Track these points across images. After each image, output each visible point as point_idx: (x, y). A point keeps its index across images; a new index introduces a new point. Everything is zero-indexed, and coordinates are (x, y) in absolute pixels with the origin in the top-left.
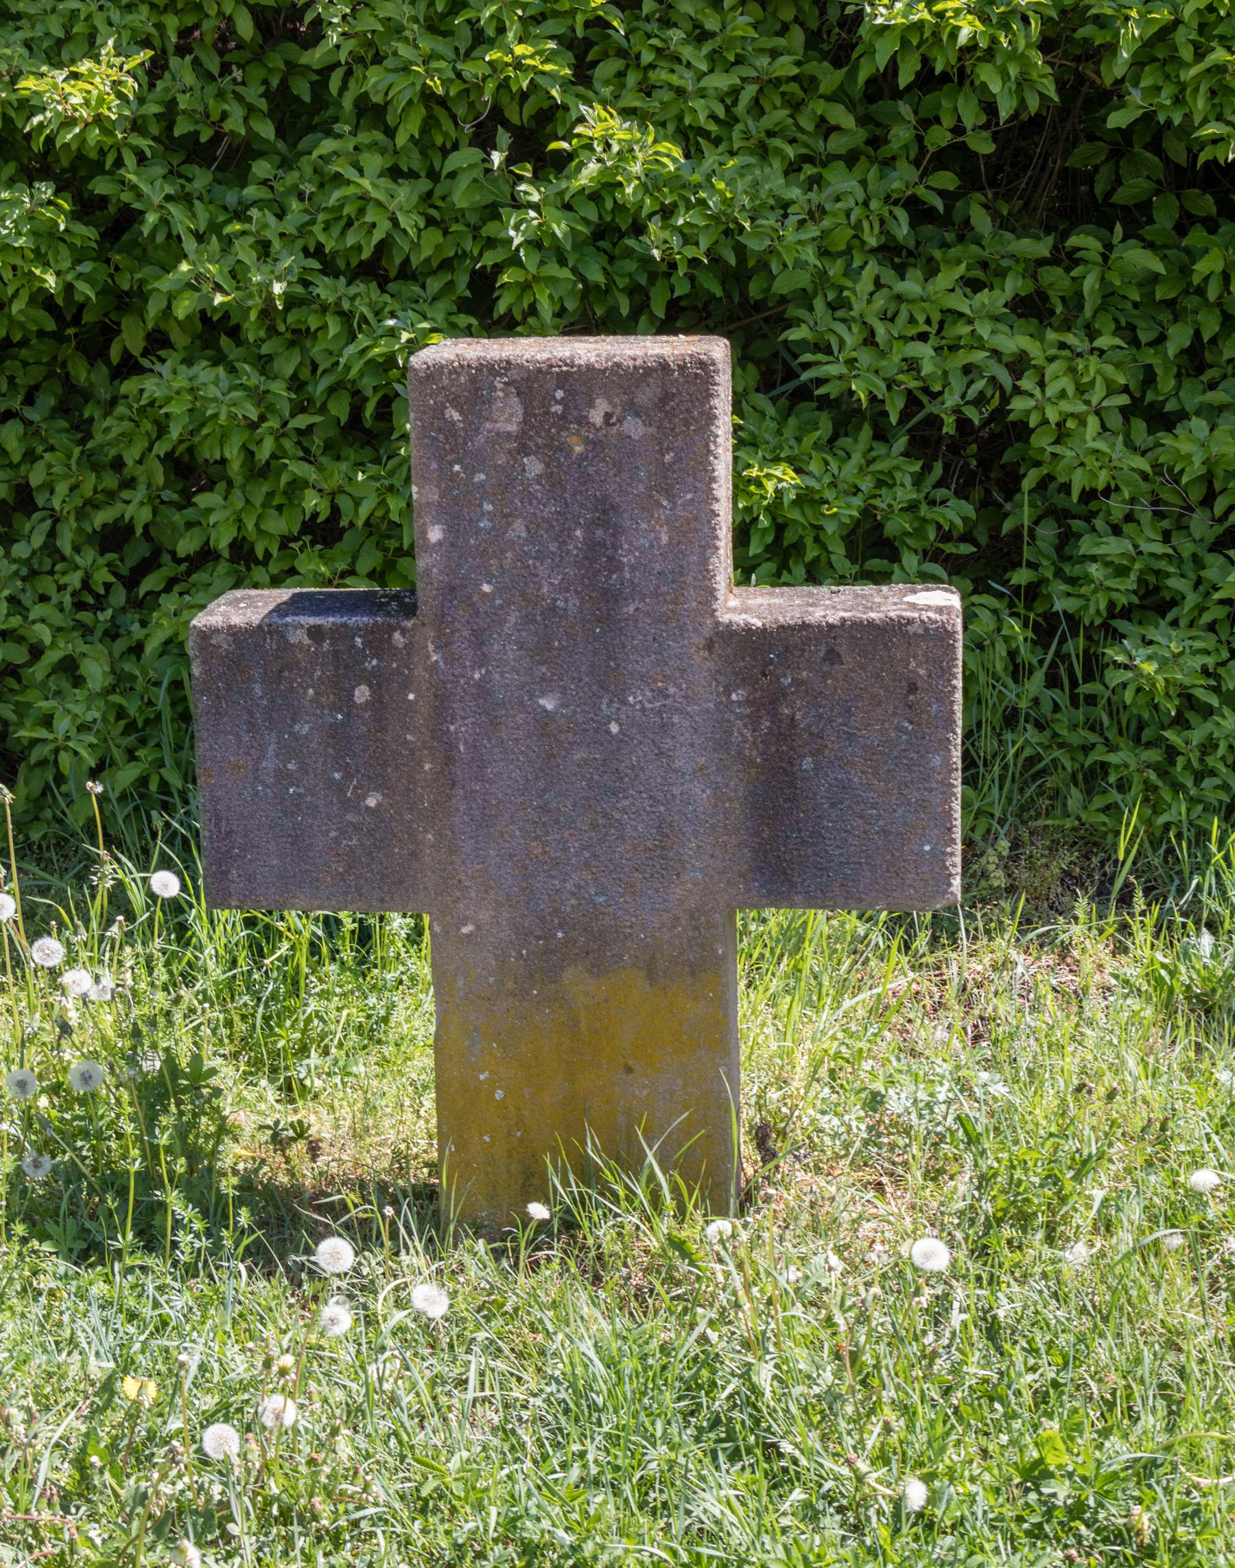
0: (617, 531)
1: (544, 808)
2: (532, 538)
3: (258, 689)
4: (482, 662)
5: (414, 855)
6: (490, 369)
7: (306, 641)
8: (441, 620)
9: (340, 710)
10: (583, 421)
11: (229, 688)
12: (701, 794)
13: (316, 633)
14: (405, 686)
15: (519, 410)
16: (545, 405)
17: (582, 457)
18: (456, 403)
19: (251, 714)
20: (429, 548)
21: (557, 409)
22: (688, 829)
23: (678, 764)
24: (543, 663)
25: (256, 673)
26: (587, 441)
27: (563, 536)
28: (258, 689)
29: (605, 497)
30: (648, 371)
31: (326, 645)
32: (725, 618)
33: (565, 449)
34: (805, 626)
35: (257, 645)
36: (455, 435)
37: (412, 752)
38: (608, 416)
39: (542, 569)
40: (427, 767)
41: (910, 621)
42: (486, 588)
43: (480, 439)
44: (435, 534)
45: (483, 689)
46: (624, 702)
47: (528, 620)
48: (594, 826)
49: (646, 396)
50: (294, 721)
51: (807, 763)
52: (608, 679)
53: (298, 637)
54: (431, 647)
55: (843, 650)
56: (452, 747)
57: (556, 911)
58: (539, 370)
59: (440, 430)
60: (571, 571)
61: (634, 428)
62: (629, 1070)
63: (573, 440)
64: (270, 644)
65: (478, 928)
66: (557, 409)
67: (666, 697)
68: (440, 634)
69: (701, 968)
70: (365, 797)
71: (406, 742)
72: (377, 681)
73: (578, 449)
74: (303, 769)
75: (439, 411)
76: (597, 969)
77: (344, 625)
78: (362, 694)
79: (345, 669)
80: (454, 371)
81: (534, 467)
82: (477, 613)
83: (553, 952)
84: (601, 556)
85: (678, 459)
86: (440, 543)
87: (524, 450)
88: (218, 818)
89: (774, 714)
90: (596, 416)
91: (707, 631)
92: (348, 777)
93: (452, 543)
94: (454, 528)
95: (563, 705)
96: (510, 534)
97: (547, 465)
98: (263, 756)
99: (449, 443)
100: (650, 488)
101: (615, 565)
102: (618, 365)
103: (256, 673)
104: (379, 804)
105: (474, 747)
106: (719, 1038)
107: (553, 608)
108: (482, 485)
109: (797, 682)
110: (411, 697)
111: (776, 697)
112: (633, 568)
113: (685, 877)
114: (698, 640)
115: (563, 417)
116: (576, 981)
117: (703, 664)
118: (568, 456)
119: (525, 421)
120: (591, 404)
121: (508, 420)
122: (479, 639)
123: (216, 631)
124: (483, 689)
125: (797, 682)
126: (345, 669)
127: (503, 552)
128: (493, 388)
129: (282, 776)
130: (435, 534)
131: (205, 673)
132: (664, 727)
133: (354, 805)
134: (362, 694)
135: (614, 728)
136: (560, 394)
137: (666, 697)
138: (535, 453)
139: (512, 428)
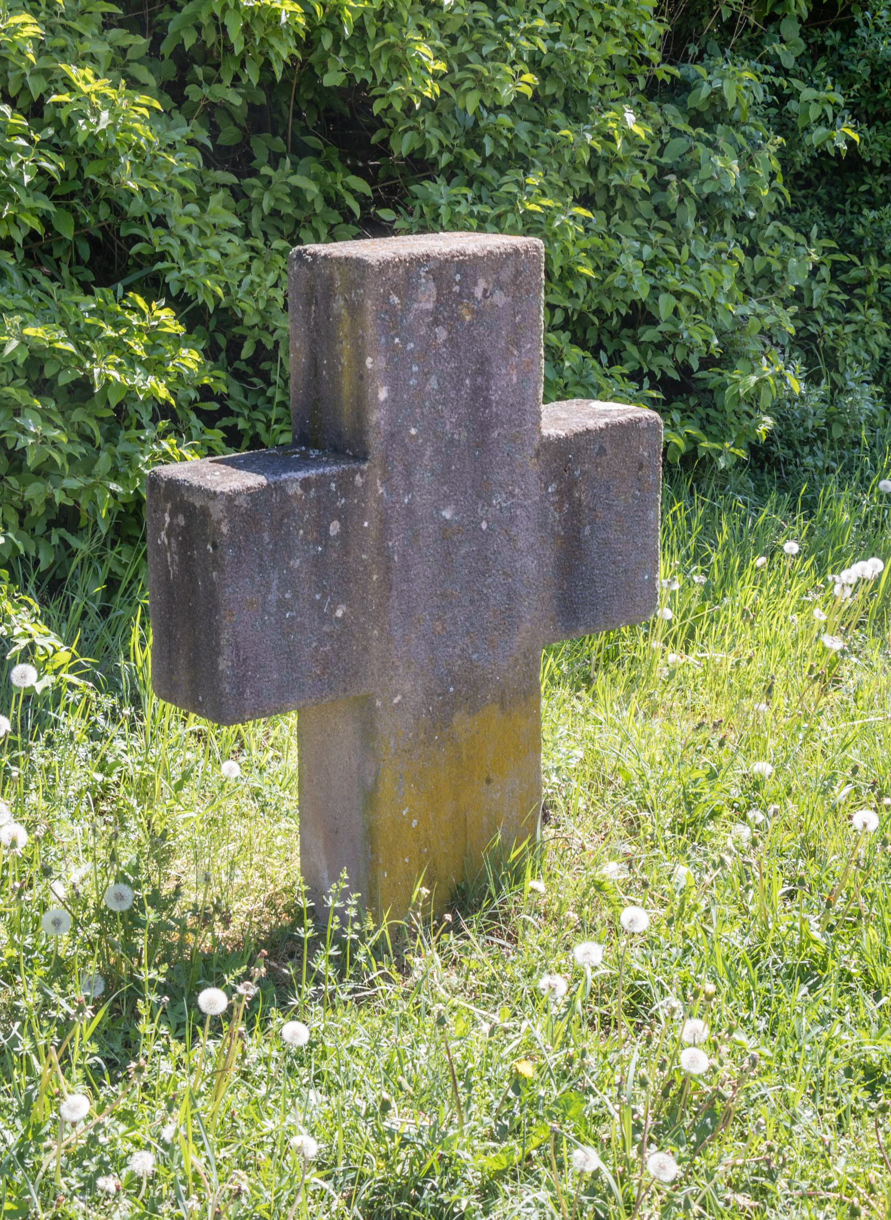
0: (488, 377)
1: (444, 596)
2: (441, 390)
3: (266, 537)
4: (409, 489)
5: (366, 649)
6: (418, 262)
7: (300, 492)
8: (386, 460)
9: (320, 544)
10: (471, 296)
11: (247, 539)
12: (531, 563)
13: (306, 484)
14: (362, 518)
15: (434, 291)
16: (449, 287)
17: (471, 324)
18: (396, 289)
19: (261, 559)
20: (378, 405)
21: (456, 289)
22: (524, 593)
23: (520, 545)
24: (443, 484)
25: (266, 523)
26: (473, 312)
27: (458, 385)
28: (266, 537)
29: (483, 352)
30: (509, 255)
31: (312, 493)
32: (545, 432)
33: (460, 318)
34: (588, 431)
35: (267, 500)
36: (395, 315)
37: (365, 567)
38: (485, 291)
39: (446, 413)
40: (375, 577)
41: (640, 420)
42: (413, 431)
43: (411, 316)
44: (383, 394)
45: (410, 510)
46: (490, 505)
47: (437, 451)
48: (472, 602)
49: (506, 275)
50: (290, 558)
51: (587, 531)
52: (482, 491)
53: (294, 489)
54: (379, 482)
55: (607, 446)
56: (390, 559)
57: (450, 672)
58: (446, 260)
59: (386, 312)
60: (463, 411)
61: (500, 299)
62: (488, 781)
63: (464, 311)
64: (276, 498)
65: (404, 697)
66: (456, 289)
67: (513, 496)
68: (385, 471)
69: (524, 696)
70: (335, 610)
71: (363, 561)
72: (344, 516)
73: (468, 318)
74: (296, 597)
75: (386, 298)
76: (473, 711)
77: (323, 475)
78: (335, 528)
79: (325, 509)
80: (396, 266)
81: (442, 334)
82: (407, 452)
83: (448, 703)
84: (480, 396)
85: (524, 319)
86: (386, 401)
87: (436, 322)
88: (237, 648)
89: (570, 496)
90: (478, 293)
91: (536, 444)
92: (324, 597)
93: (393, 400)
94: (394, 390)
95: (457, 514)
96: (428, 388)
97: (450, 333)
98: (269, 591)
99: (392, 321)
100: (507, 343)
101: (487, 403)
102: (491, 252)
103: (266, 523)
104: (344, 614)
105: (403, 556)
106: (532, 742)
107: (452, 441)
108: (412, 351)
109: (583, 473)
110: (366, 524)
111: (573, 484)
112: (498, 403)
113: (522, 628)
114: (531, 452)
115: (460, 295)
116: (461, 722)
117: (533, 467)
118: (462, 324)
119: (438, 301)
120: (475, 284)
121: (428, 301)
122: (408, 472)
123: (238, 494)
124: (410, 510)
125: (583, 473)
126: (325, 509)
127: (424, 401)
128: (419, 277)
129: (282, 605)
130: (383, 394)
131: (231, 530)
132: (512, 519)
133: (326, 618)
134: (335, 528)
135: (484, 526)
136: (458, 277)
137: (513, 496)
138: (443, 324)
139: (430, 306)
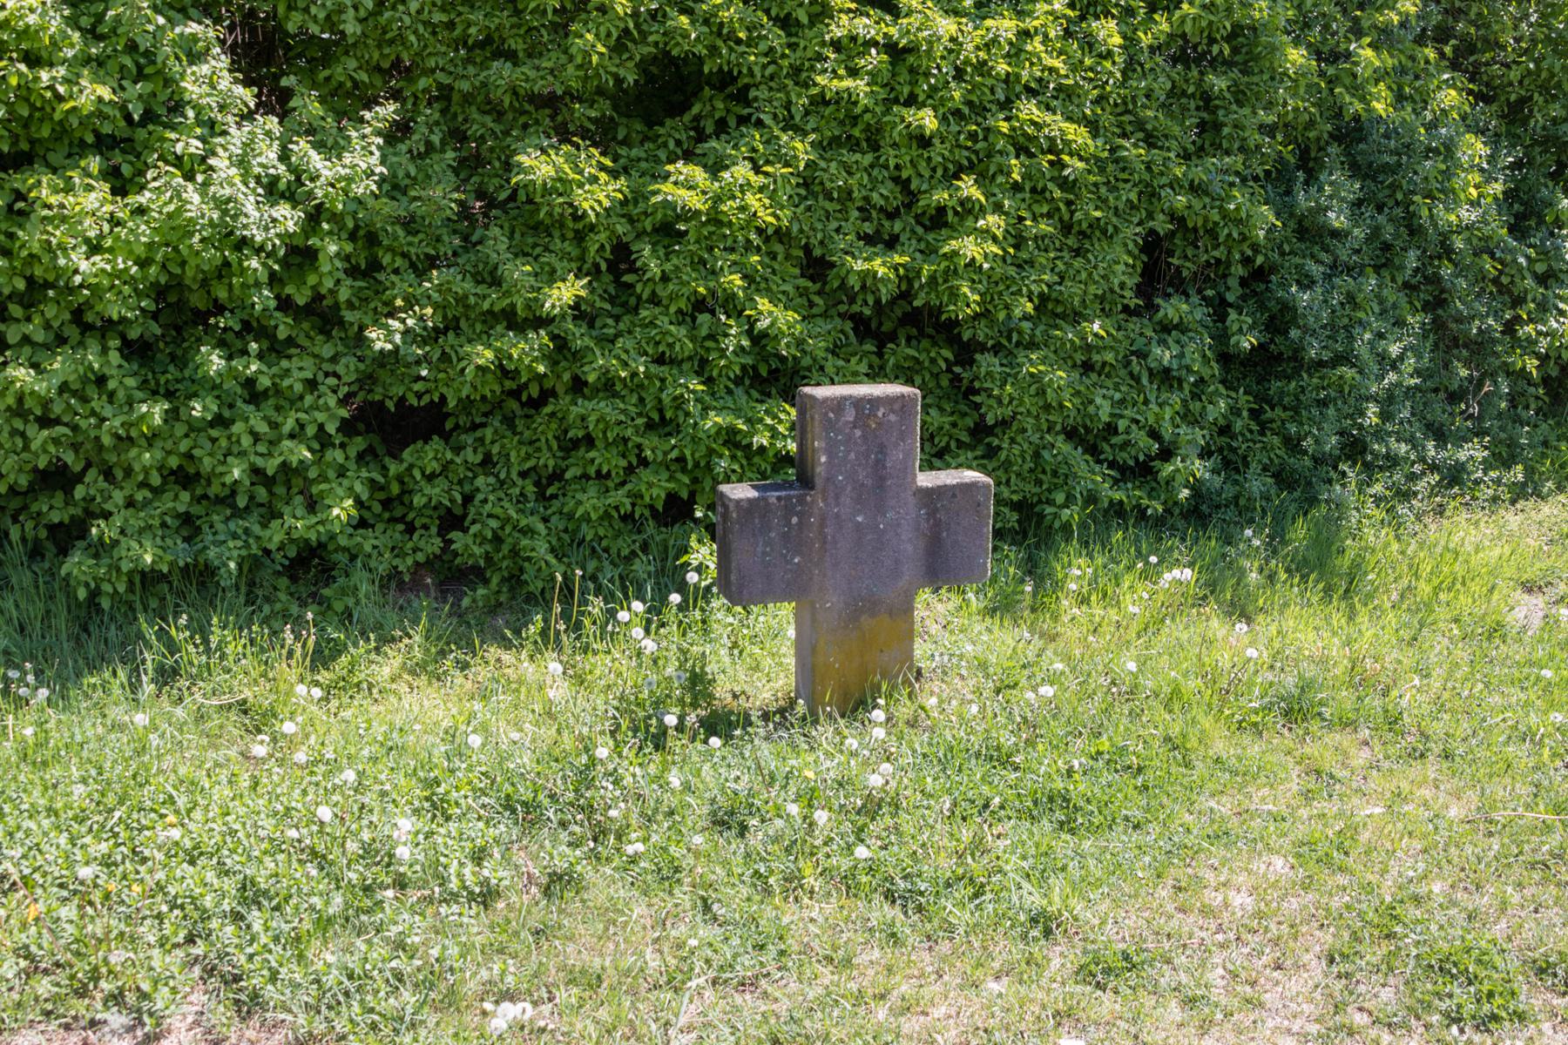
0: (885, 455)
4: (838, 505)
6: (844, 398)
8: (824, 491)
12: (910, 548)
13: (779, 498)
27: (867, 457)
44: (823, 459)
45: (837, 516)
49: (896, 407)
52: (881, 509)
53: (773, 500)
61: (893, 418)
72: (800, 515)
78: (795, 520)
79: (789, 510)
81: (858, 433)
84: (879, 464)
90: (880, 414)
93: (829, 462)
94: (830, 457)
99: (829, 426)
101: (884, 467)
111: (935, 511)
116: (865, 620)
117: (912, 501)
122: (837, 497)
124: (837, 516)
126: (789, 510)
129: (764, 553)
130: (823, 459)
132: (899, 525)
133: (790, 562)
134: (795, 520)
